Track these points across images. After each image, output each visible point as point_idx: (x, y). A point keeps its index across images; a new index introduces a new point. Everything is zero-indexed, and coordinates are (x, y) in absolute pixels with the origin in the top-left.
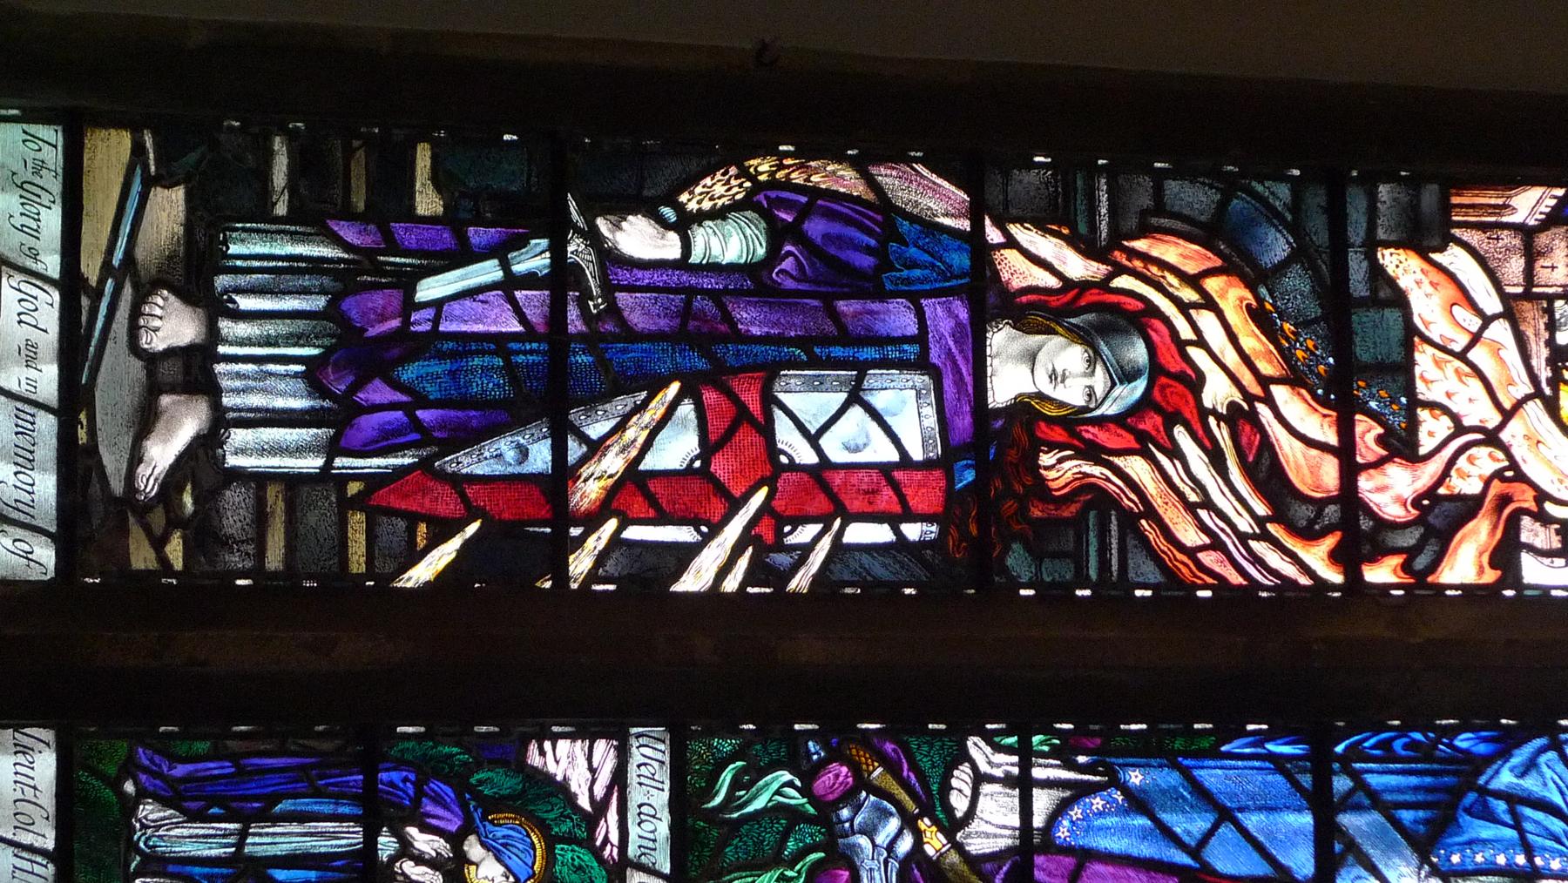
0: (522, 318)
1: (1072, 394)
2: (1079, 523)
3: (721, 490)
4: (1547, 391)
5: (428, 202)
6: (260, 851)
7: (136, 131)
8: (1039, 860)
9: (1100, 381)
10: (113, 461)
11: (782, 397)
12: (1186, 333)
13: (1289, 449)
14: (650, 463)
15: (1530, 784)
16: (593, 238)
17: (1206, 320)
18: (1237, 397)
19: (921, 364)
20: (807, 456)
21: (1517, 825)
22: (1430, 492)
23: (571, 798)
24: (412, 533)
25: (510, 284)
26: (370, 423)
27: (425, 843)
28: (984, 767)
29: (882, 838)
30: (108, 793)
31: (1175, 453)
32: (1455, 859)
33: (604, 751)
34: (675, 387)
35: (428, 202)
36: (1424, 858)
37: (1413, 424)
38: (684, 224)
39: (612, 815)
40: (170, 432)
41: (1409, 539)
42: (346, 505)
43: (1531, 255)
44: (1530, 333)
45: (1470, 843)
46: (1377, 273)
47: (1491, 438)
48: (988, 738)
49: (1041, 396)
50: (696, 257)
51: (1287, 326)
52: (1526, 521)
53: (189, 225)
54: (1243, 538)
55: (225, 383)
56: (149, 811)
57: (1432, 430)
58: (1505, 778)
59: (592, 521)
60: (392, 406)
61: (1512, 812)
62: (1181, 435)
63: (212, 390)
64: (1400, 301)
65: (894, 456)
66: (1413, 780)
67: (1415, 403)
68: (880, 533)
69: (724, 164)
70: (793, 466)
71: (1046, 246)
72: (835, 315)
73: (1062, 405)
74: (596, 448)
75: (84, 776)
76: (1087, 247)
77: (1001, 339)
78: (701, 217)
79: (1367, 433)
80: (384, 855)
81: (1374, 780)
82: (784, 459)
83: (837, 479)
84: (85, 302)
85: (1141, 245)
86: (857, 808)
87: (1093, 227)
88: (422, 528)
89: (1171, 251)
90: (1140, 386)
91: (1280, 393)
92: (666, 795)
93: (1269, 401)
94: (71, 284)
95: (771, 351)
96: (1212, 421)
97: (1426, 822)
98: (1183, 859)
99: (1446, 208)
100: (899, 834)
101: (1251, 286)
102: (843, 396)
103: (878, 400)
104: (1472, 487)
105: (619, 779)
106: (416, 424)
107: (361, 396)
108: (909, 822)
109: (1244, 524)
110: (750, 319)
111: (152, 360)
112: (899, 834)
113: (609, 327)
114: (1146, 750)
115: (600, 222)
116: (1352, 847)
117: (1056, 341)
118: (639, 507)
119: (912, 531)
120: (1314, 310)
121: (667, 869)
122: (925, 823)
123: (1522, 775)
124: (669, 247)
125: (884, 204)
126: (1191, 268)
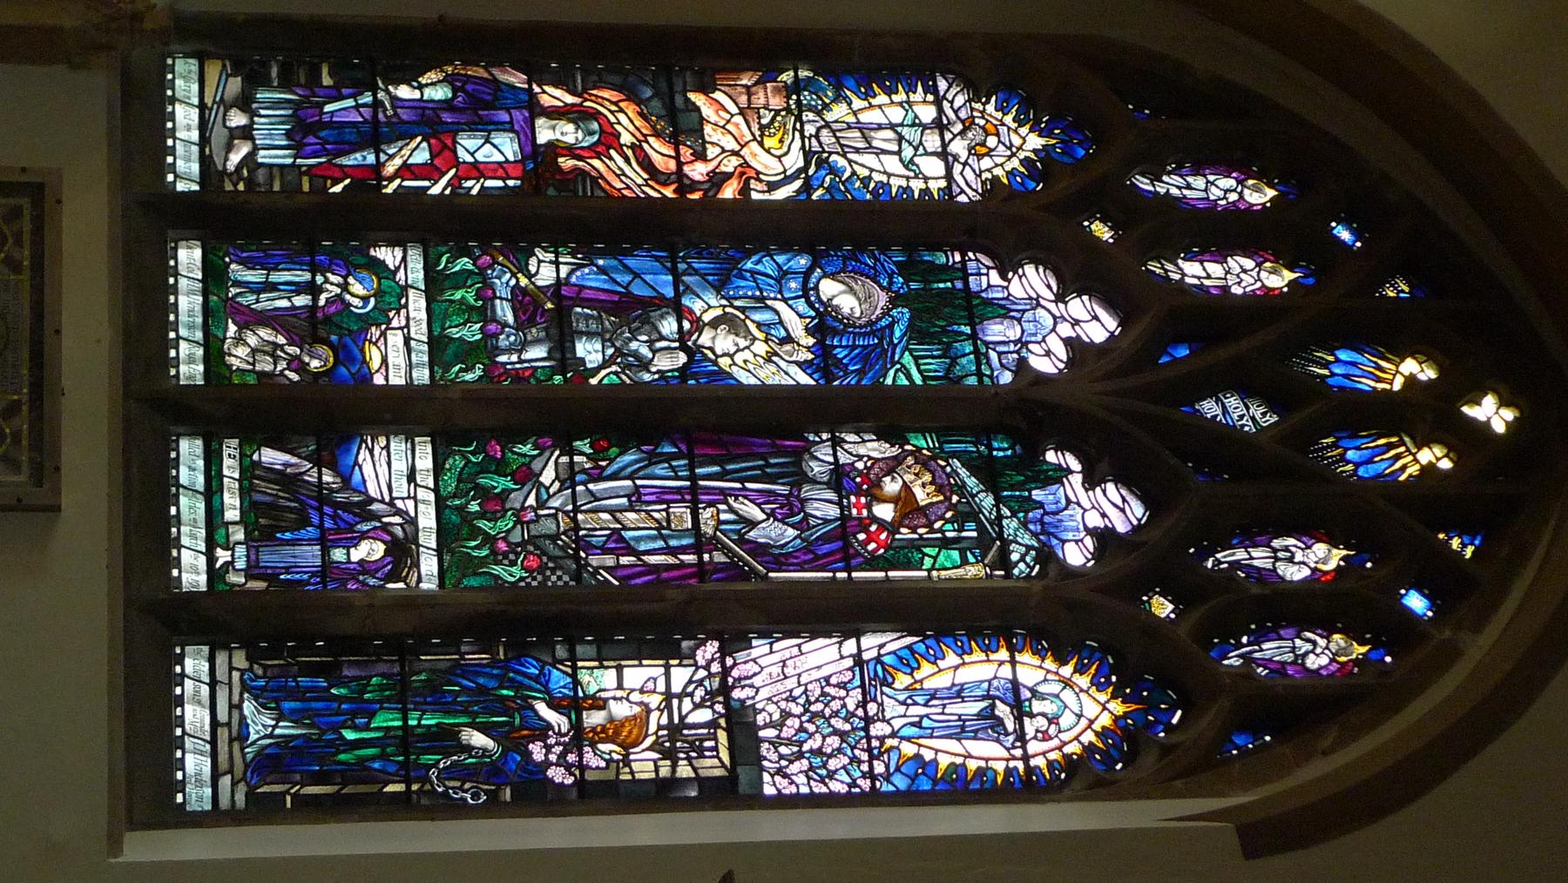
0: (363, 117)
1: (570, 139)
2: (575, 183)
3: (437, 169)
4: (759, 139)
5: (327, 81)
6: (274, 280)
7: (223, 60)
8: (563, 288)
9: (580, 135)
10: (218, 161)
11: (460, 141)
12: (613, 119)
13: (656, 158)
14: (410, 161)
15: (759, 267)
16: (387, 92)
17: (621, 117)
18: (635, 141)
19: (512, 130)
20: (469, 159)
21: (755, 281)
22: (713, 171)
23: (387, 266)
24: (326, 183)
25: (357, 107)
26: (308, 149)
27: (332, 278)
28: (541, 258)
29: (504, 280)
30: (221, 262)
31: (611, 158)
32: (731, 293)
33: (398, 252)
34: (419, 139)
35: (327, 81)
36: (718, 292)
37: (705, 149)
38: (421, 87)
39: (402, 270)
40: (238, 150)
41: (706, 186)
42: (301, 174)
43: (749, 95)
44: (751, 120)
45: (737, 287)
46: (688, 100)
47: (735, 153)
48: (543, 248)
49: (557, 140)
50: (425, 98)
51: (654, 118)
52: (752, 181)
53: (242, 89)
54: (639, 186)
55: (257, 137)
56: (233, 266)
57: (712, 152)
58: (749, 265)
59: (391, 179)
60: (317, 144)
61: (752, 276)
62: (612, 152)
63: (252, 139)
64: (698, 109)
65: (503, 159)
66: (712, 266)
67: (705, 142)
68: (499, 183)
69: (436, 68)
70: (464, 162)
71: (558, 93)
72: (478, 116)
73: (565, 143)
74: (391, 157)
75: (211, 256)
76: (573, 93)
77: (540, 122)
78: (427, 85)
79: (686, 153)
80: (319, 283)
81: (695, 265)
82: (461, 160)
83: (481, 166)
84: (207, 112)
85: (594, 92)
86: (494, 270)
87: (575, 87)
88: (329, 182)
89: (606, 94)
90: (596, 137)
91: (651, 139)
92: (422, 265)
93: (647, 142)
94: (202, 106)
95: (456, 127)
96: (625, 148)
97: (718, 280)
98: (623, 290)
99: (715, 80)
100: (510, 279)
101: (638, 105)
102: (483, 141)
103: (495, 141)
104: (730, 169)
105: (404, 259)
106: (325, 149)
107: (305, 141)
108: (514, 275)
109: (640, 181)
110: (447, 117)
111: (231, 129)
112: (510, 279)
113: (394, 120)
114: (602, 254)
115: (390, 87)
116: (688, 288)
117: (563, 122)
118: (408, 175)
119: (511, 183)
120: (663, 113)
121: (423, 288)
122: (519, 275)
123: (756, 265)
124: (416, 95)
125: (495, 80)
126: (614, 99)
